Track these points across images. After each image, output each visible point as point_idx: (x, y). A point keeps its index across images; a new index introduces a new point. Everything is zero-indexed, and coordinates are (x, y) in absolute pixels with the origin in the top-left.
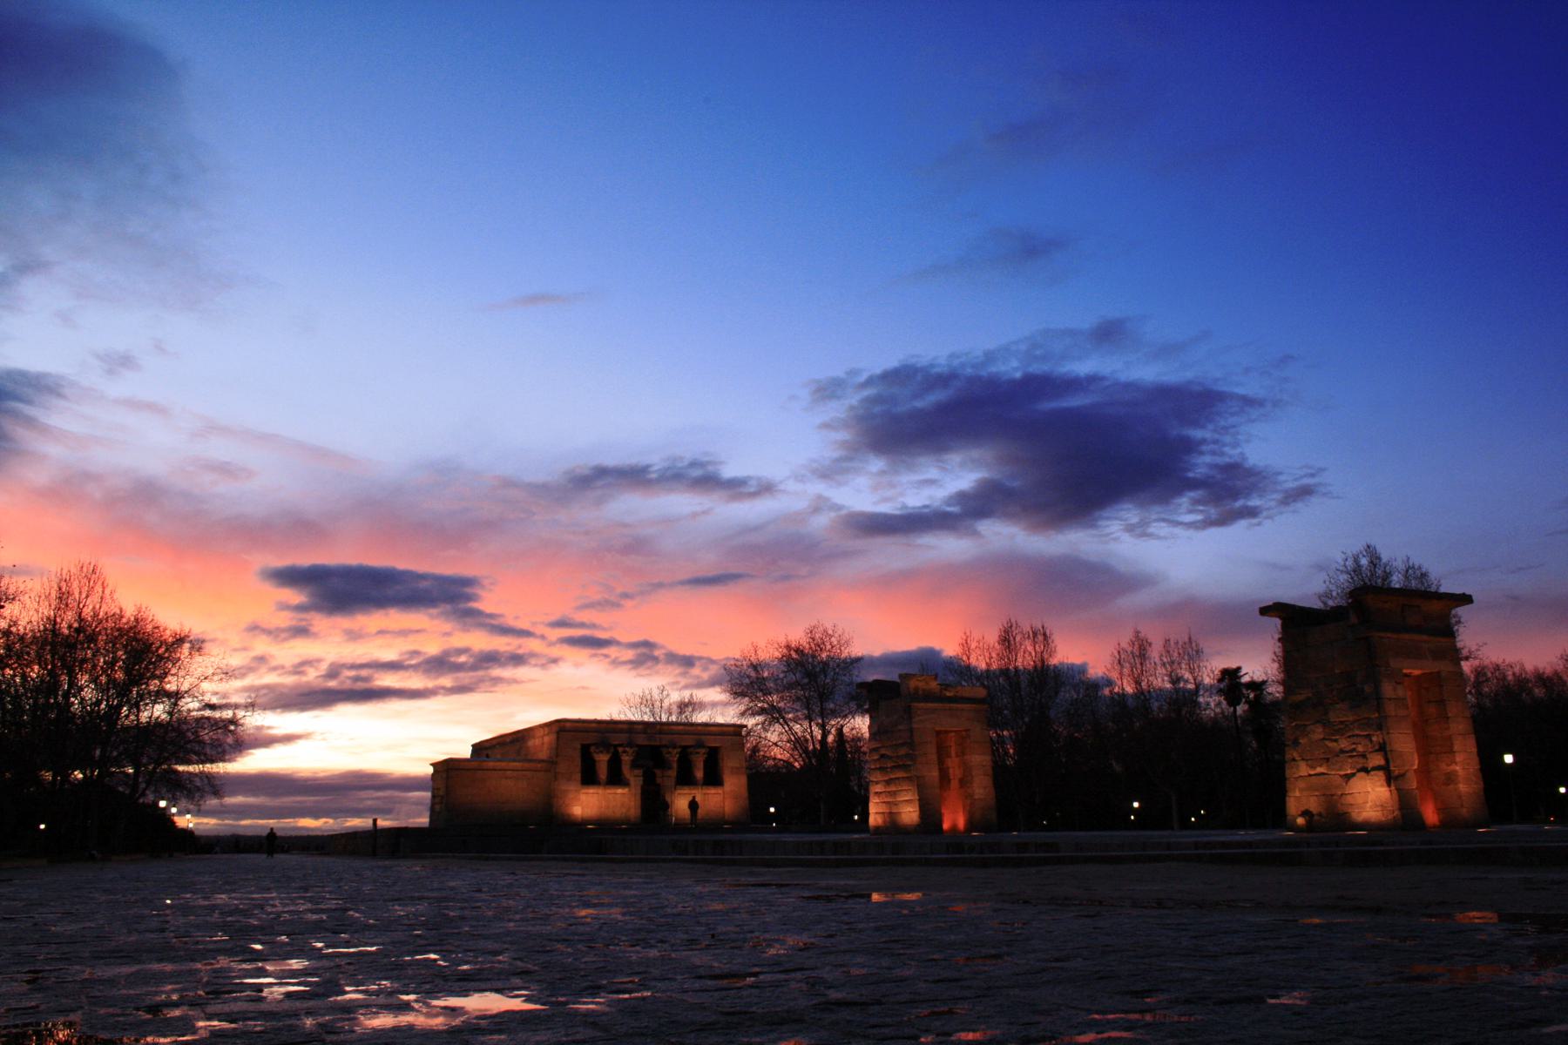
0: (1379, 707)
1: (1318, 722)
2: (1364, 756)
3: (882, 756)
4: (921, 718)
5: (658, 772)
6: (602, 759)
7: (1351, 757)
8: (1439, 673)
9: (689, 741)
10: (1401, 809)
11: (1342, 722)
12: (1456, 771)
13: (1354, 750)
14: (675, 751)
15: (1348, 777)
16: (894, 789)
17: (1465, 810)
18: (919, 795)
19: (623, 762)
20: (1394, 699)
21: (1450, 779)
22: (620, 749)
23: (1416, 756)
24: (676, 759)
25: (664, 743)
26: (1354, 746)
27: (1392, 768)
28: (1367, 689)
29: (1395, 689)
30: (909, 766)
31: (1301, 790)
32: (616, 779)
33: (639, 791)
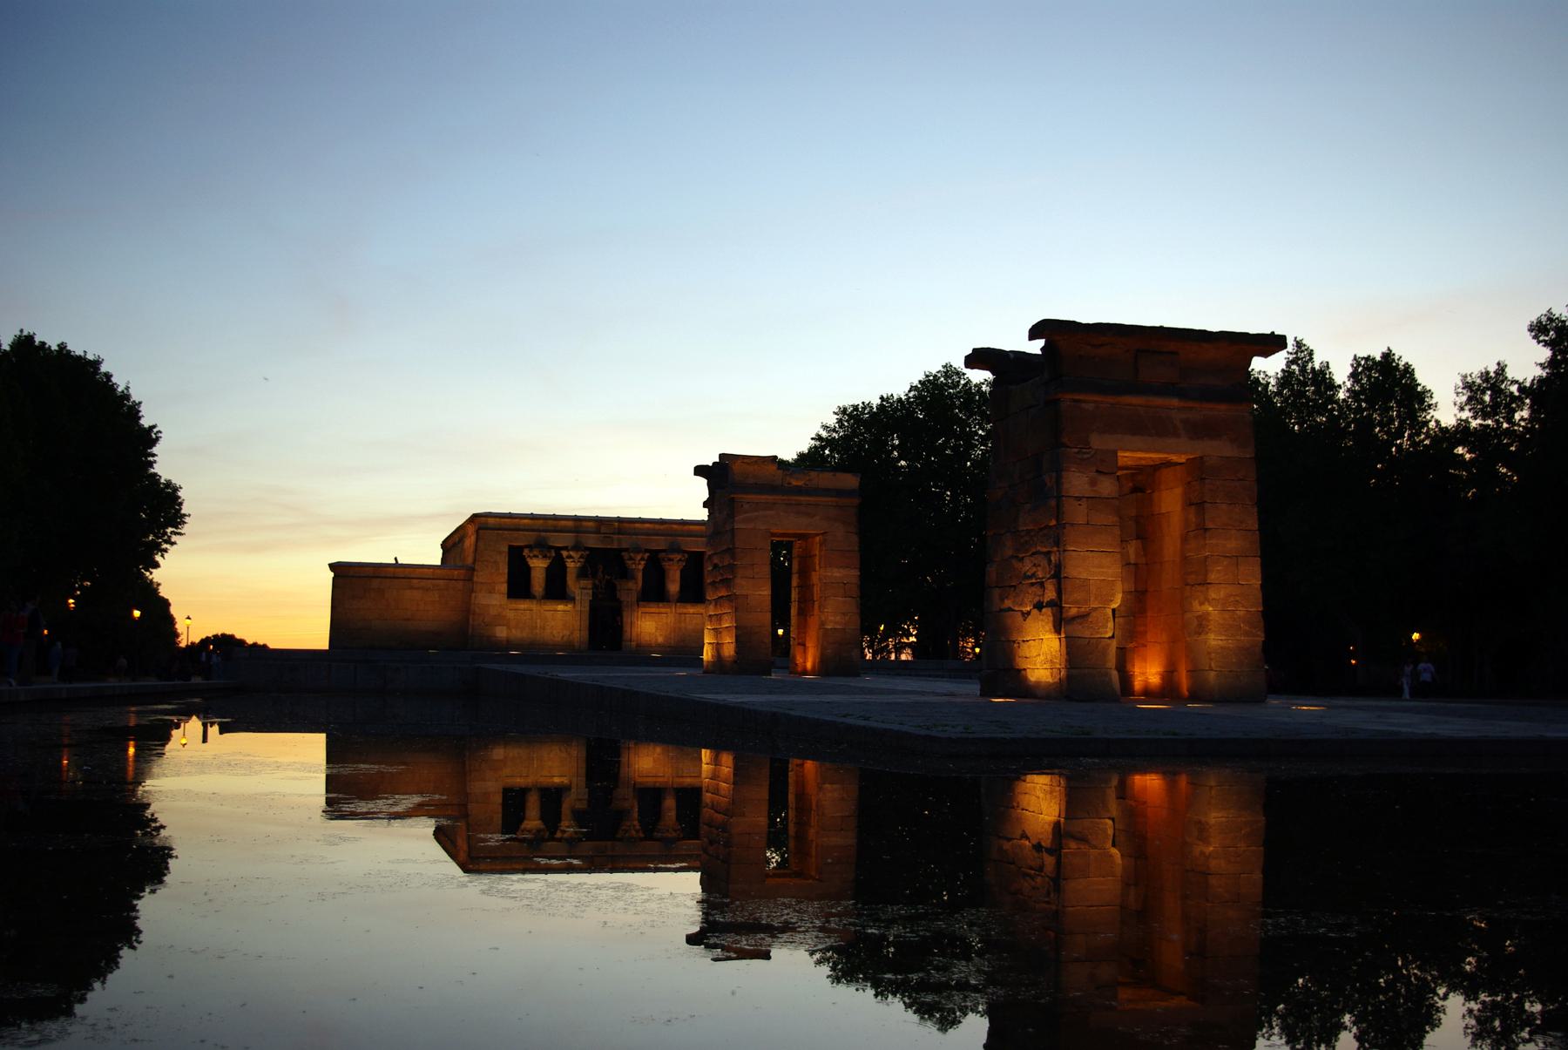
0: (1058, 513)
3: (715, 566)
6: (538, 565)
7: (1032, 584)
8: (1201, 458)
9: (659, 543)
11: (1028, 532)
12: (1208, 614)
13: (1033, 575)
15: (1026, 615)
16: (720, 612)
17: (1212, 674)
19: (568, 570)
21: (1202, 623)
22: (565, 553)
23: (1119, 586)
24: (641, 567)
25: (624, 546)
26: (1034, 569)
29: (1093, 483)
30: (730, 579)
32: (556, 590)
33: (588, 609)
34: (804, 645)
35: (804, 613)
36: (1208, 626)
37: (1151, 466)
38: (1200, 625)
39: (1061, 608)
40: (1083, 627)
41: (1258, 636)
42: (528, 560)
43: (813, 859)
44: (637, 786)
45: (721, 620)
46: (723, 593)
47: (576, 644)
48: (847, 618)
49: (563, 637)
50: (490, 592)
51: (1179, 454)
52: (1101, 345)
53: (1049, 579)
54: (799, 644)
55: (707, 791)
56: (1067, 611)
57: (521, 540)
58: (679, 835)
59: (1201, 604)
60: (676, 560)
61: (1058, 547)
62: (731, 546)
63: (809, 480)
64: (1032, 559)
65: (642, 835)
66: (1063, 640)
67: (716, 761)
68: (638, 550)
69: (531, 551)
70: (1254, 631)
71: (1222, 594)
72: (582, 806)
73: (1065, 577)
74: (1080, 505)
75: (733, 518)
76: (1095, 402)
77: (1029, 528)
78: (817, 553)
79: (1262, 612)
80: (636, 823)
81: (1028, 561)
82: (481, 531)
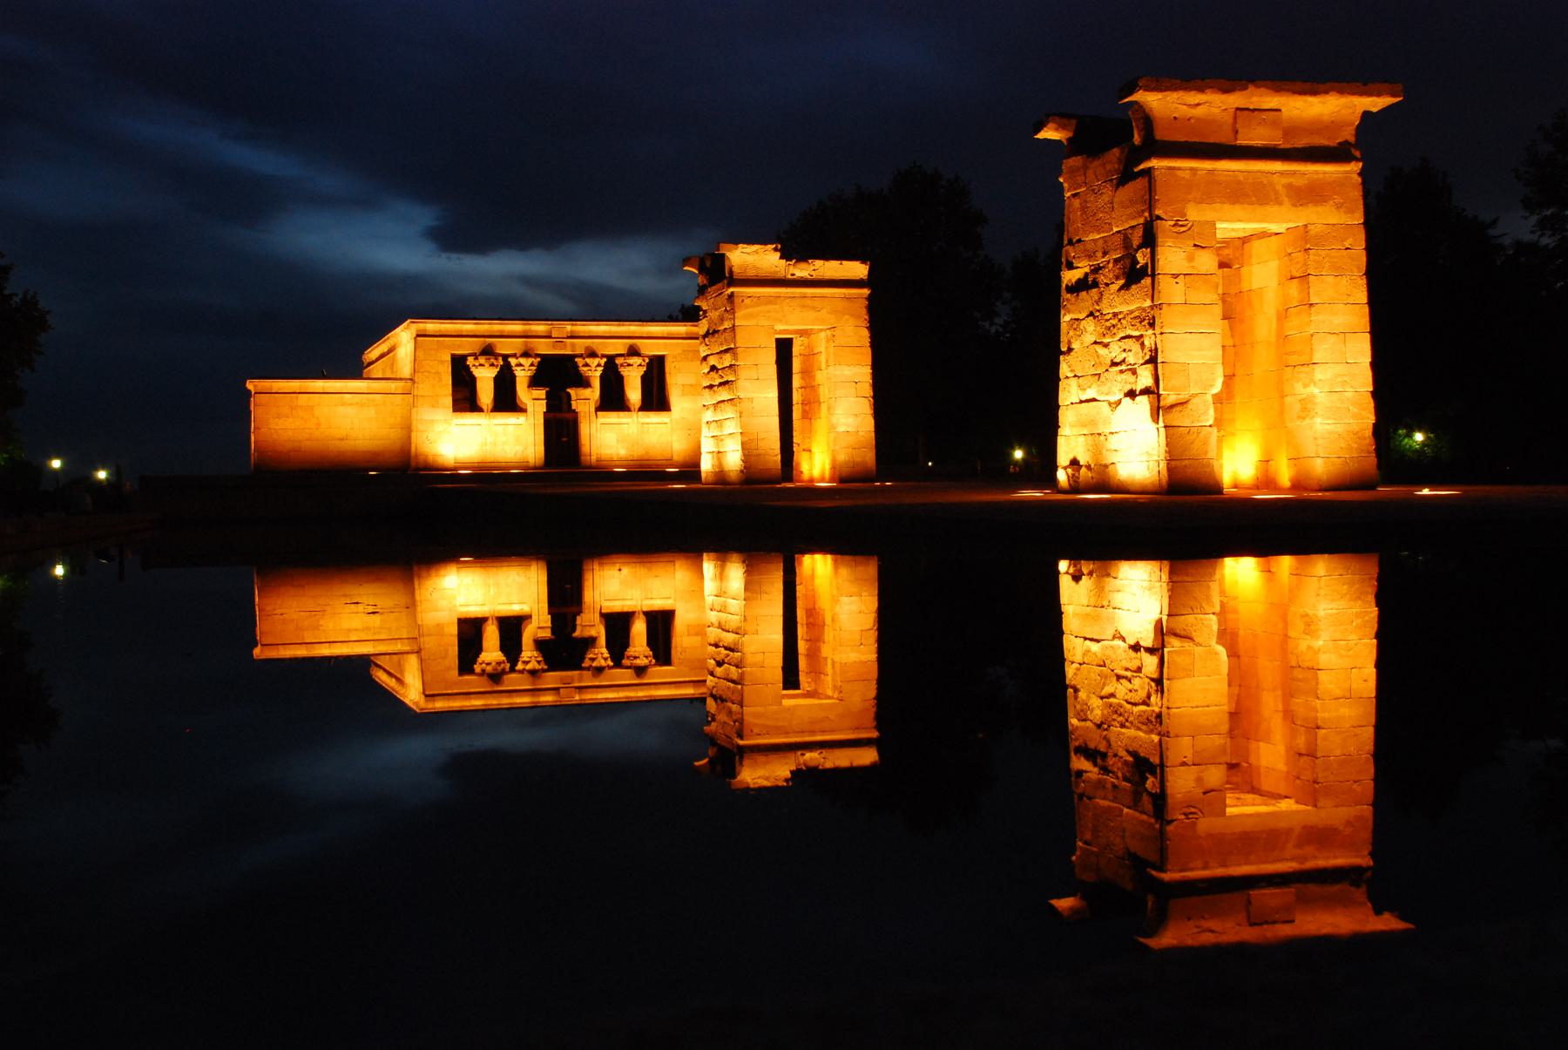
1: (1091, 314)
2: (1134, 372)
3: (713, 368)
4: (749, 310)
5: (568, 390)
6: (485, 376)
7: (1122, 372)
9: (618, 347)
10: (1169, 461)
11: (1115, 315)
12: (1313, 396)
13: (1124, 360)
14: (595, 362)
16: (721, 418)
18: (741, 428)
19: (517, 379)
20: (1185, 275)
21: (1307, 408)
22: (513, 361)
24: (598, 374)
26: (1124, 355)
27: (1161, 392)
28: (1142, 258)
29: (1191, 258)
31: (1072, 426)
32: (506, 401)
34: (810, 451)
35: (806, 415)
36: (1314, 409)
37: (1239, 238)
38: (1304, 409)
39: (1159, 396)
40: (1183, 416)
41: (1369, 418)
42: (473, 369)
43: (829, 678)
44: (603, 611)
45: (721, 426)
46: (724, 394)
47: (530, 461)
48: (860, 419)
49: (515, 455)
50: (433, 406)
51: (1279, 221)
52: (1198, 105)
53: (1142, 365)
54: (804, 450)
55: (711, 610)
56: (1165, 399)
57: (465, 347)
58: (651, 661)
59: (1306, 386)
60: (635, 366)
61: (1154, 329)
62: (732, 346)
63: (814, 270)
64: (1120, 343)
65: (611, 664)
66: (1162, 430)
67: (721, 576)
68: (593, 354)
69: (476, 359)
70: (1363, 413)
71: (1329, 375)
72: (547, 634)
73: (1163, 362)
74: (1177, 283)
75: (734, 313)
76: (1191, 169)
77: (1116, 310)
78: (823, 350)
79: (1371, 392)
80: (604, 650)
81: (1116, 347)
82: (419, 339)
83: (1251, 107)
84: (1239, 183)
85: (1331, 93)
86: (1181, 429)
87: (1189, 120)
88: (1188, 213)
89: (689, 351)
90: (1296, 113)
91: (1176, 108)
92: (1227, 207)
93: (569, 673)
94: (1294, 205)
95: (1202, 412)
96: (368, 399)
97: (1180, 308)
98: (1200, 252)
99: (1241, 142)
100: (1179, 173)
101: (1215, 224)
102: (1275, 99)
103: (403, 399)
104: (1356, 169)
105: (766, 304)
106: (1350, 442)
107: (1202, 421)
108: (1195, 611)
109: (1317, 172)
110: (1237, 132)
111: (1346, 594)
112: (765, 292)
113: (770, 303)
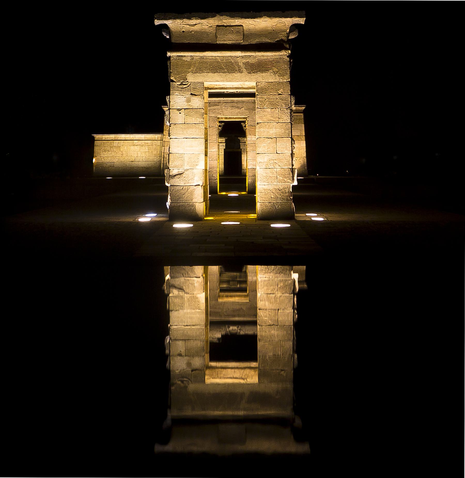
5: (239, 138)
20: (185, 109)
29: (188, 101)
33: (223, 153)
41: (288, 182)
52: (196, 25)
56: (172, 171)
70: (285, 180)
74: (180, 113)
76: (191, 56)
83: (225, 25)
84: (218, 62)
85: (264, 17)
86: (178, 187)
87: (191, 32)
88: (188, 78)
89: (297, 119)
90: (251, 27)
91: (184, 27)
92: (210, 74)
93: (235, 274)
94: (249, 73)
95: (190, 178)
96: (145, 143)
97: (181, 126)
98: (194, 98)
99: (220, 42)
100: (184, 58)
101: (203, 83)
102: (236, 21)
103: (161, 143)
104: (285, 53)
105: (213, 106)
106: (277, 195)
107: (191, 183)
108: (185, 276)
109: (263, 56)
110: (216, 37)
111: (274, 270)
112: (212, 100)
113: (216, 105)
